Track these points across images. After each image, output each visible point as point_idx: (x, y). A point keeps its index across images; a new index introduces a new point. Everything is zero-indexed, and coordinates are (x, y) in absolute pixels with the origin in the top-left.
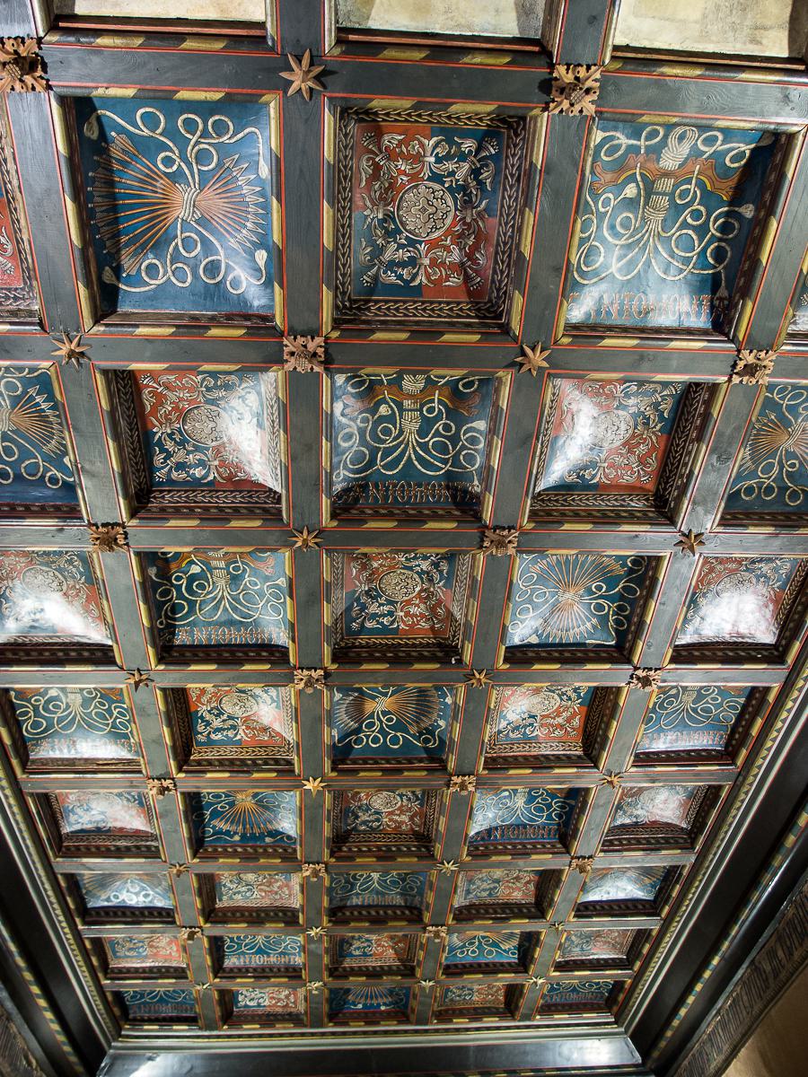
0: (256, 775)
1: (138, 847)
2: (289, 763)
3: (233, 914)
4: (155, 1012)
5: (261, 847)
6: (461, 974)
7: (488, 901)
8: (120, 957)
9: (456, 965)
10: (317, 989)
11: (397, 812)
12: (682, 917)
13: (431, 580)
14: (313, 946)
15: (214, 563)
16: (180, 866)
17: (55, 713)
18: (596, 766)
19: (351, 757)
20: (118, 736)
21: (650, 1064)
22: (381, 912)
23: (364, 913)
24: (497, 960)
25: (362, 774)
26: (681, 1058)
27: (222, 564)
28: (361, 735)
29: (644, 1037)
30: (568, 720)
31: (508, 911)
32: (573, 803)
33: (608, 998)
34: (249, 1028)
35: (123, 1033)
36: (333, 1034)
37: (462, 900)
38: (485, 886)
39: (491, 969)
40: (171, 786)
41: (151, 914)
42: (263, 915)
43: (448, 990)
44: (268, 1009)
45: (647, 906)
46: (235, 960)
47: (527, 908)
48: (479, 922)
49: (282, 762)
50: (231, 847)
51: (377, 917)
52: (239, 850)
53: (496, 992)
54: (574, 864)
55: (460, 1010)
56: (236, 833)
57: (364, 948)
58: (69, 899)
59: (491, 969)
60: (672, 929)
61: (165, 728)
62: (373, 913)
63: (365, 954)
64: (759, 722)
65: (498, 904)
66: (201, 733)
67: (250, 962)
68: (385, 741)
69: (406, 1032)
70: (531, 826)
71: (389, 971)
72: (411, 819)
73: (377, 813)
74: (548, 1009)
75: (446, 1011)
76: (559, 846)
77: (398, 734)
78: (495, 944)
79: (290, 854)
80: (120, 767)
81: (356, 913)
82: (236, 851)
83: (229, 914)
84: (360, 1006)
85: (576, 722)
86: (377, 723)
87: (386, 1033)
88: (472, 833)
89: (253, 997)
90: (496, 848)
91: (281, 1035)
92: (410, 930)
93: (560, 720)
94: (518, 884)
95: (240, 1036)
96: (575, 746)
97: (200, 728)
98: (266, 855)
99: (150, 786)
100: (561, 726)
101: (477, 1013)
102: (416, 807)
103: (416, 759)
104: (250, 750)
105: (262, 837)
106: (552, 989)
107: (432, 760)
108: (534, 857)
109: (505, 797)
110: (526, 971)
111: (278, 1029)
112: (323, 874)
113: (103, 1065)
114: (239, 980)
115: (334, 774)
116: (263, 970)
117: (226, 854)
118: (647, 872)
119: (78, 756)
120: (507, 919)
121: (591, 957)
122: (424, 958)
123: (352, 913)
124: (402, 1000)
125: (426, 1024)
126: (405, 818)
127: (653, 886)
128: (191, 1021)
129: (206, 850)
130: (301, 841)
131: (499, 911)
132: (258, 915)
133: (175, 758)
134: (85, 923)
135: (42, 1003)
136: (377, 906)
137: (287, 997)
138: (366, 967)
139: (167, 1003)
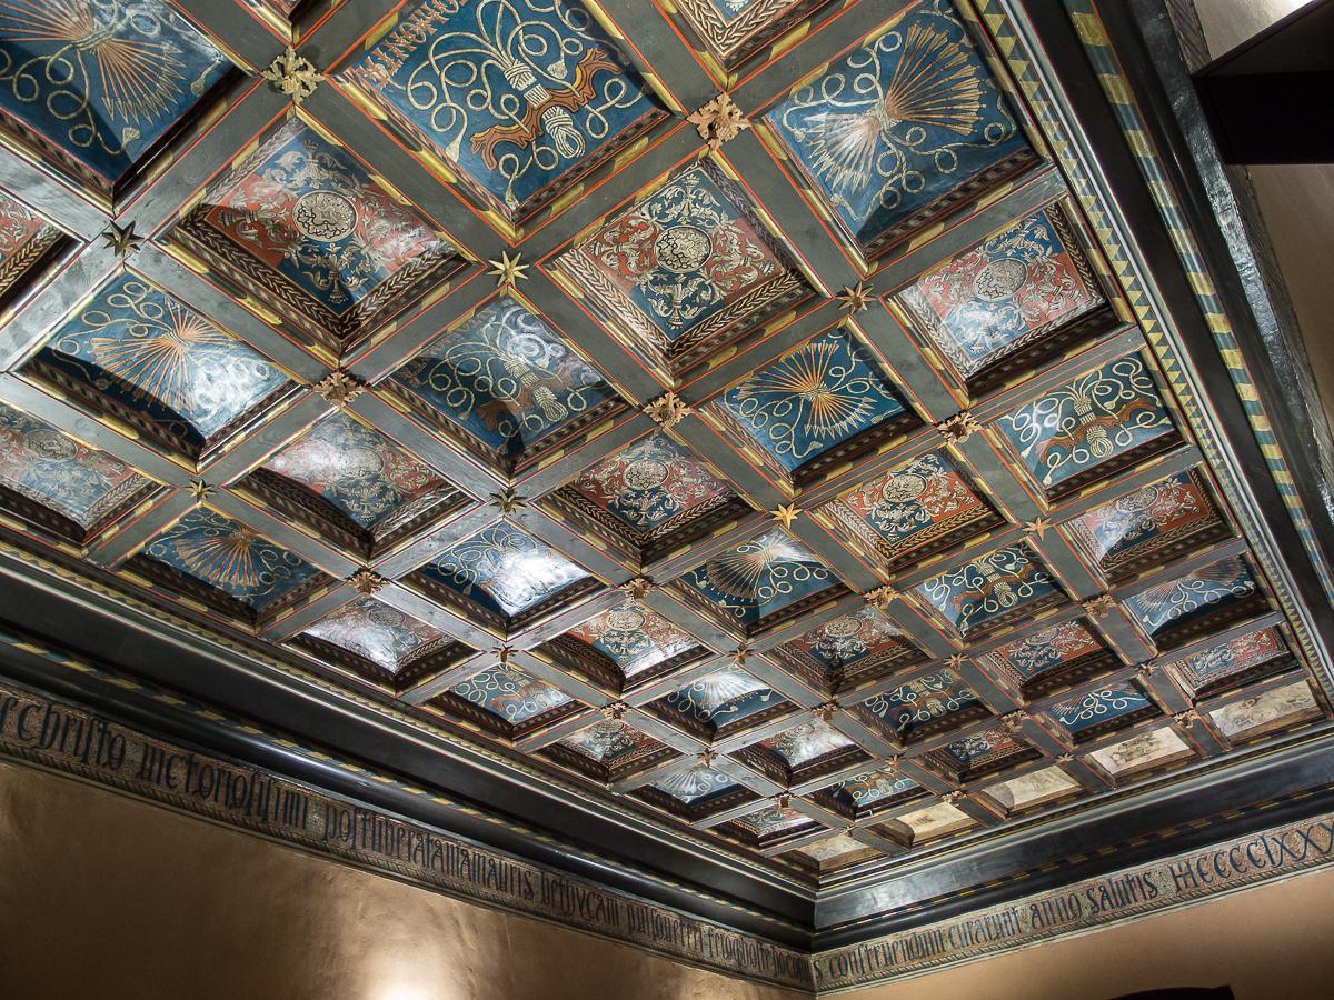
13: (825, 641)
15: (997, 577)
17: (1102, 383)
27: (990, 579)
64: (476, 729)
102: (612, 498)
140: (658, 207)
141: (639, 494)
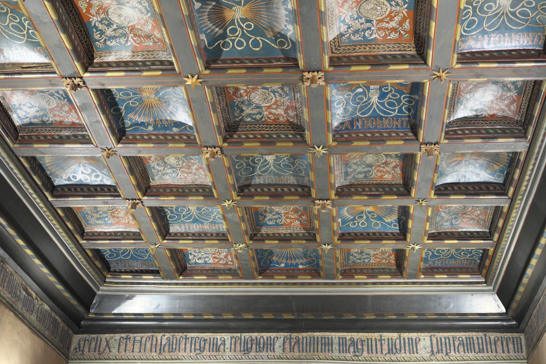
0: (145, 74)
1: (76, 136)
2: (171, 63)
3: (164, 190)
4: (129, 266)
5: (169, 135)
6: (353, 240)
7: (365, 181)
8: (91, 224)
9: (349, 234)
10: (241, 249)
11: (275, 107)
12: (523, 195)
14: (229, 216)
16: (109, 150)
18: (426, 63)
19: (222, 58)
20: (34, 45)
21: (511, 313)
22: (279, 189)
23: (266, 190)
24: (382, 231)
25: (230, 71)
26: (531, 307)
28: (227, 40)
29: (505, 294)
30: (401, 23)
31: (380, 190)
32: (417, 97)
33: (480, 264)
34: (199, 279)
35: (107, 280)
36: (262, 284)
37: (342, 180)
38: (360, 169)
39: (376, 237)
40: (81, 84)
41: (102, 190)
42: (187, 191)
43: (349, 254)
44: (213, 266)
45: (498, 188)
46: (178, 227)
47: (397, 188)
48: (357, 198)
49: (166, 63)
50: (147, 135)
51: (277, 193)
52: (153, 137)
53: (389, 256)
54: (423, 150)
55: (361, 269)
56: (149, 124)
57: (276, 219)
58: (35, 178)
59: (376, 237)
60: (517, 206)
61: (62, 35)
62: (273, 190)
63: (277, 224)
65: (373, 184)
66: (98, 41)
67: (189, 228)
68: (248, 44)
69: (318, 284)
70: (387, 118)
71: (297, 237)
72: (286, 111)
73: (258, 107)
74: (430, 271)
75: (350, 270)
76: (411, 134)
77: (258, 38)
78: (380, 218)
79: (192, 140)
80: (39, 69)
81: (259, 190)
82: (150, 138)
83: (161, 190)
84: (283, 265)
85: (407, 25)
86: (239, 29)
87: (302, 284)
88: (335, 124)
89: (201, 255)
90: (358, 136)
91: (223, 284)
92: (306, 202)
93: (393, 24)
94: (388, 169)
95: (192, 284)
96: (409, 47)
97: (97, 36)
98: (174, 140)
99: (65, 84)
100: (394, 30)
101: (373, 272)
103: (275, 59)
104: (140, 54)
105: (169, 127)
106: (433, 256)
107: (287, 59)
108: (389, 143)
109: (360, 93)
110: (405, 239)
111: (221, 279)
112: (219, 156)
113: (94, 302)
114: (181, 242)
115: (207, 72)
116: (200, 234)
117: (143, 141)
118: (494, 158)
119: (7, 61)
120: (380, 195)
121: (460, 230)
122: (319, 226)
123: (256, 190)
124: (314, 261)
125: (334, 279)
126: (280, 111)
127: (501, 171)
128: (155, 273)
129: (128, 138)
130: (197, 129)
131: (374, 189)
132: (184, 191)
133: (79, 59)
134: (53, 196)
135: (29, 252)
136: (275, 185)
137: (226, 257)
138: (278, 234)
139: (137, 260)
140: (173, 175)
141: (274, 92)
